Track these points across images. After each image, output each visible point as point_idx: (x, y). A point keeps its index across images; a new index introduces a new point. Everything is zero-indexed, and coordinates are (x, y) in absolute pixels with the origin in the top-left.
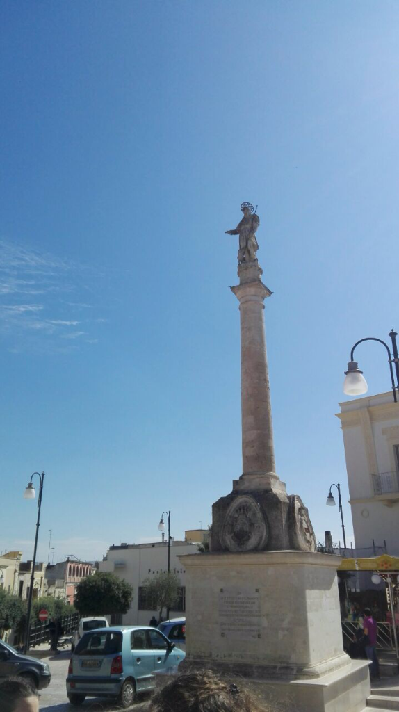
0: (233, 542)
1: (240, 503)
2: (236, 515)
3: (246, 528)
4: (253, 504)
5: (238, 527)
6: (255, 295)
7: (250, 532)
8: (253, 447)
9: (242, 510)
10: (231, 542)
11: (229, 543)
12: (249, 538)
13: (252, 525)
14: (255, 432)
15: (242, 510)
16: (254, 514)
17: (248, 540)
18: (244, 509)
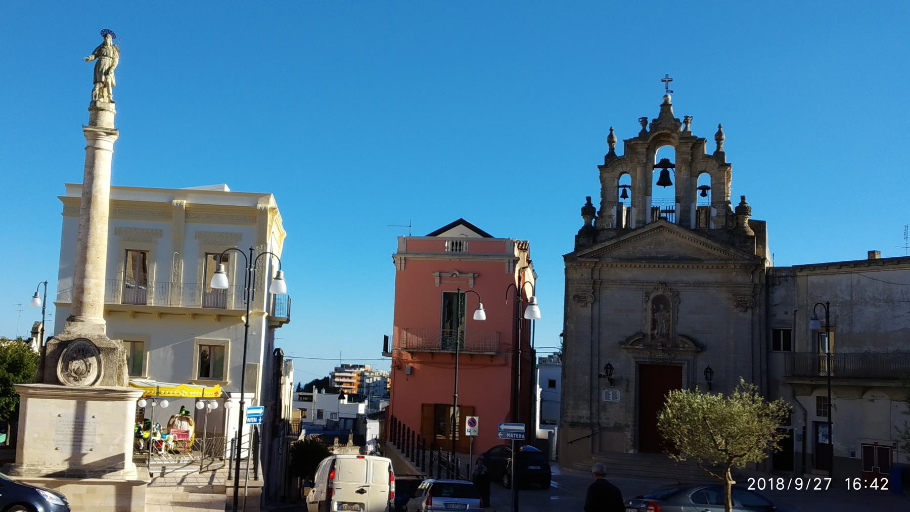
1: (78, 345)
9: (81, 352)
15: (81, 352)
18: (83, 351)
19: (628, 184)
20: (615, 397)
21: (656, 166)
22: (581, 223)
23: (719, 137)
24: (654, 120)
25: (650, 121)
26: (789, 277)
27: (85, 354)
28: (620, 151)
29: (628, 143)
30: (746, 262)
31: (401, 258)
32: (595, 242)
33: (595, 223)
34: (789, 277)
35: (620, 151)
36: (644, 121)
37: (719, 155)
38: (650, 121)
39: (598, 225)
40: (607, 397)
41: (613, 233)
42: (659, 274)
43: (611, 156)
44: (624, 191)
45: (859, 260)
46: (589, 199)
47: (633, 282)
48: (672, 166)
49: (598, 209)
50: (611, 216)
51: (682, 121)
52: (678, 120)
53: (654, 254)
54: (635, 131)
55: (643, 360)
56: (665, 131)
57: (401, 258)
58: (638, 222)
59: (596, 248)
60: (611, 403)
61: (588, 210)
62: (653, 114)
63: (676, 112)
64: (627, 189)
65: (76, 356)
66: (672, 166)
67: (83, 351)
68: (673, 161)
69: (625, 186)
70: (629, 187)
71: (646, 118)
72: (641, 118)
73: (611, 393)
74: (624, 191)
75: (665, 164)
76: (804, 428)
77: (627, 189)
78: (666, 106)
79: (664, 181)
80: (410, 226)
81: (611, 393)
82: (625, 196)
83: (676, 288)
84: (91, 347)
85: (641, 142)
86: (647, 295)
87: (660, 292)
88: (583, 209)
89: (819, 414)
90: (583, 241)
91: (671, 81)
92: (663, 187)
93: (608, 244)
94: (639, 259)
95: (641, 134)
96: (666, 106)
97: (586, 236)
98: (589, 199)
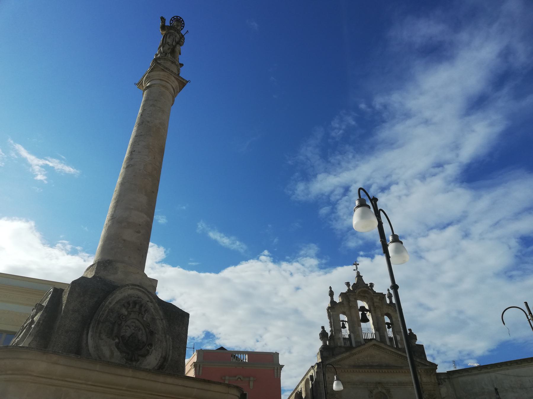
0: (117, 353)
2: (124, 312)
3: (142, 336)
4: (150, 304)
5: (127, 332)
6: (174, 90)
7: (151, 345)
8: (138, 232)
9: (137, 307)
10: (112, 353)
12: (148, 353)
13: (152, 333)
14: (145, 216)
16: (153, 319)
17: (144, 356)
18: (141, 306)
21: (360, 310)
22: (320, 344)
25: (351, 284)
26: (446, 379)
27: (143, 313)
28: (337, 299)
29: (342, 295)
30: (428, 367)
31: (200, 365)
32: (334, 355)
34: (446, 379)
36: (348, 284)
38: (351, 284)
39: (332, 344)
42: (376, 377)
43: (333, 302)
44: (343, 324)
45: (497, 363)
46: (323, 328)
48: (367, 311)
49: (329, 334)
51: (369, 285)
52: (367, 284)
54: (345, 289)
56: (365, 289)
57: (200, 365)
58: (356, 342)
59: (338, 358)
61: (323, 335)
62: (353, 281)
63: (367, 281)
64: (345, 323)
65: (126, 313)
66: (367, 311)
67: (141, 306)
68: (367, 307)
69: (343, 321)
70: (346, 321)
71: (349, 282)
72: (346, 283)
75: (363, 309)
77: (345, 323)
78: (359, 277)
79: (366, 320)
80: (194, 348)
84: (150, 304)
85: (352, 294)
86: (371, 392)
87: (380, 389)
88: (321, 334)
91: (359, 265)
93: (344, 355)
95: (349, 290)
96: (359, 277)
97: (325, 352)
98: (323, 328)
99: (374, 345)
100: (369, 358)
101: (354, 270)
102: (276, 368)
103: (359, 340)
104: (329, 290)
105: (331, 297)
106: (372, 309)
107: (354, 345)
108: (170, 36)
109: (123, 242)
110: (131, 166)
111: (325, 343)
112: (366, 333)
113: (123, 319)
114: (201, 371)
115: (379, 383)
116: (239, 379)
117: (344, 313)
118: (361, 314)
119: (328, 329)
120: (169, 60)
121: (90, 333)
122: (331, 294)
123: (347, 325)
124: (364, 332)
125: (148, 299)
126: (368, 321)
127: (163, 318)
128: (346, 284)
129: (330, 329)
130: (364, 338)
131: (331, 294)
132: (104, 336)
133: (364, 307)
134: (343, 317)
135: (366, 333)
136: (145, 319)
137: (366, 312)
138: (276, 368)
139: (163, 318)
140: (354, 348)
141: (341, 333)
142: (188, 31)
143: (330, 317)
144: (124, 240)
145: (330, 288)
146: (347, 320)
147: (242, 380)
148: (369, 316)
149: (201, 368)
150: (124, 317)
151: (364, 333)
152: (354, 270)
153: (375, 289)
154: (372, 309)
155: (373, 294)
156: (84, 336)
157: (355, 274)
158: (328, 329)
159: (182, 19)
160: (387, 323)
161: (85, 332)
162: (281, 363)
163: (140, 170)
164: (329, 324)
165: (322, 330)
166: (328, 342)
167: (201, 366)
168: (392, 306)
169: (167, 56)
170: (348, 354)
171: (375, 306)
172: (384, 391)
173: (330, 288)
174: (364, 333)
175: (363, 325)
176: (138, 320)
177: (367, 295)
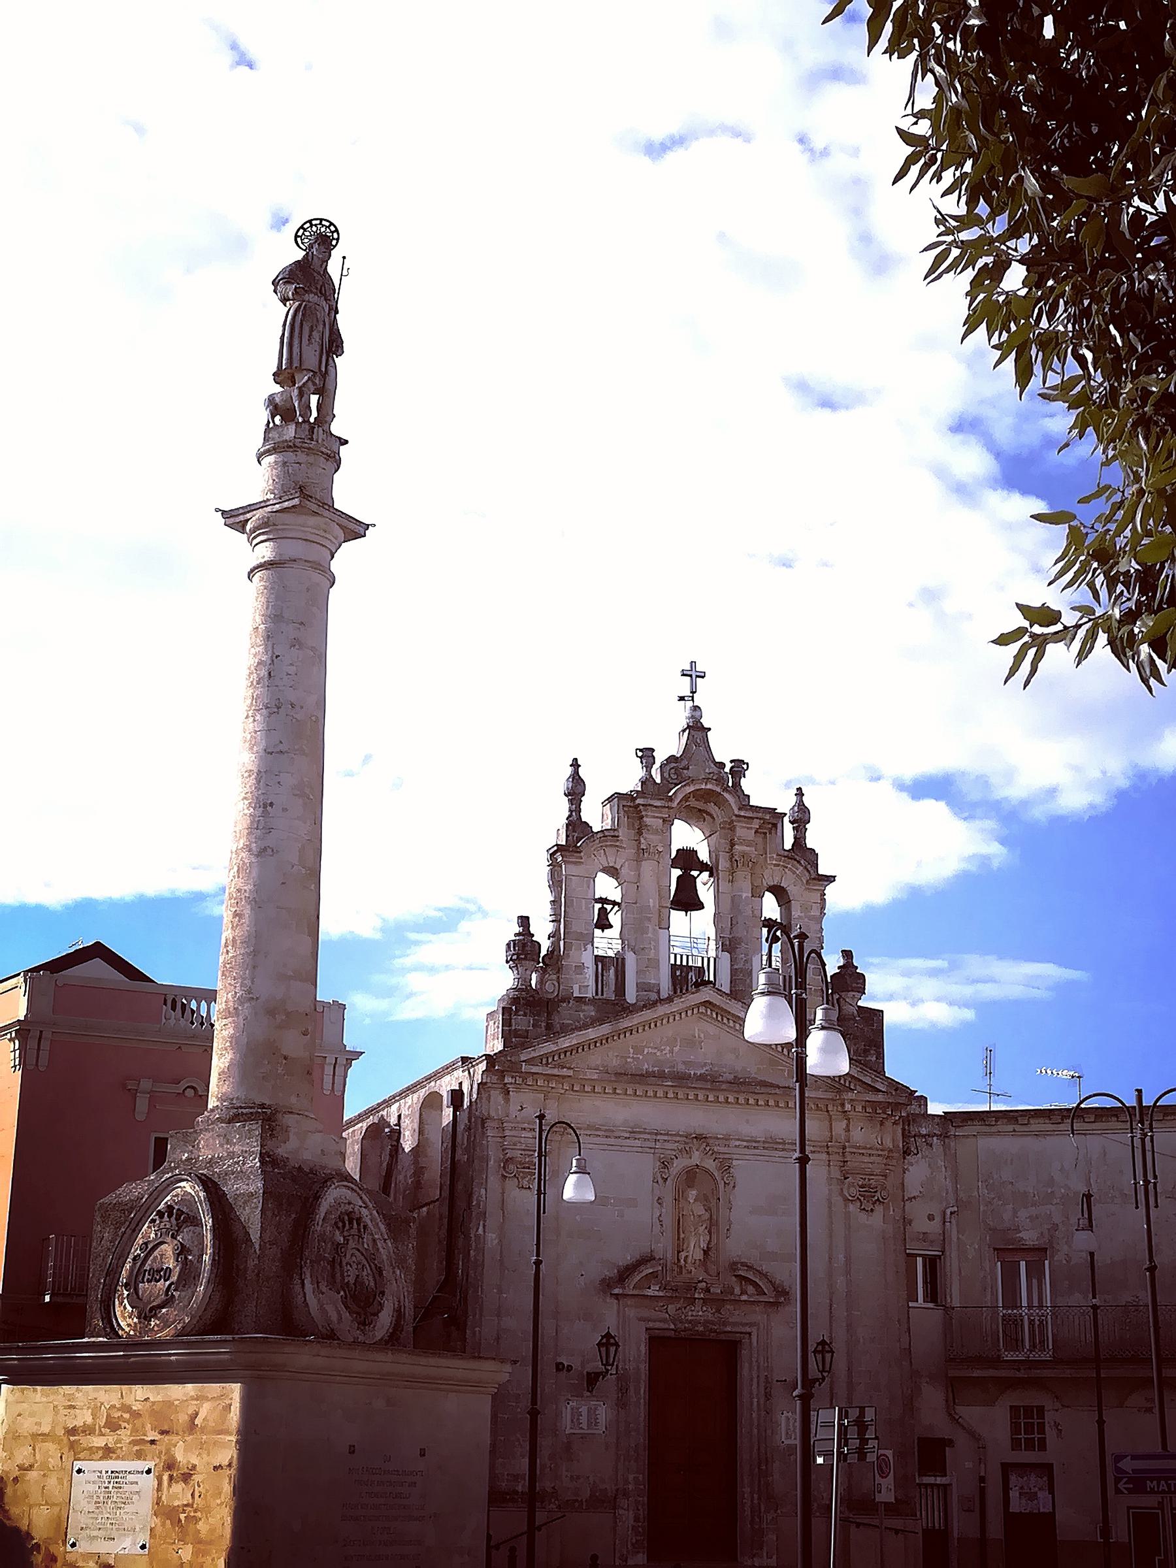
4: (365, 1212)
11: (334, 1317)
17: (376, 1314)
19: (611, 898)
20: (593, 1421)
22: (504, 980)
23: (801, 818)
24: (672, 759)
25: (660, 757)
26: (935, 1138)
28: (595, 815)
29: (620, 801)
30: (880, 1097)
32: (552, 1032)
33: (541, 981)
34: (935, 1138)
35: (595, 815)
36: (646, 755)
37: (804, 855)
38: (660, 757)
39: (549, 986)
40: (576, 1414)
41: (590, 1010)
43: (576, 825)
46: (524, 921)
47: (634, 1132)
48: (703, 867)
49: (543, 952)
50: (580, 968)
52: (722, 765)
53: (681, 1068)
54: (629, 778)
55: (662, 1325)
56: (709, 786)
58: (641, 987)
59: (565, 1042)
60: (583, 1437)
62: (669, 745)
63: (723, 750)
66: (703, 867)
68: (704, 855)
70: (614, 903)
71: (653, 750)
73: (584, 1410)
74: (603, 913)
75: (687, 859)
76: (982, 1479)
78: (696, 730)
79: (688, 901)
81: (584, 1410)
82: (604, 924)
83: (725, 1150)
86: (665, 1165)
87: (696, 1158)
89: (1016, 1445)
90: (522, 1022)
92: (684, 913)
93: (592, 1033)
94: (641, 1077)
95: (647, 781)
96: (696, 730)
98: (524, 921)
99: (707, 1004)
100: (676, 1049)
101: (682, 699)
102: (331, 1060)
103: (653, 981)
104: (569, 771)
105: (571, 801)
106: (723, 864)
107: (631, 996)
108: (311, 330)
109: (284, 1061)
110: (269, 850)
111: (524, 980)
112: (682, 956)
113: (342, 1253)
114: (44, 1055)
115: (699, 1137)
116: (190, 1092)
117: (612, 872)
118: (679, 878)
119: (542, 931)
120: (322, 452)
121: (309, 1286)
122: (576, 790)
123: (615, 918)
124: (677, 950)
125: (361, 1203)
126: (699, 906)
127: (386, 1237)
128: (640, 754)
129: (550, 928)
130: (672, 962)
131: (576, 790)
132: (324, 1289)
133: (694, 852)
134: (606, 887)
135: (682, 956)
136: (366, 1246)
137: (695, 873)
138: (331, 1060)
139: (386, 1237)
140: (630, 1010)
141: (589, 946)
142: (344, 258)
143: (555, 882)
144: (285, 1058)
145: (575, 764)
146: (619, 900)
147: (201, 1096)
148: (705, 890)
149: (45, 1045)
150: (343, 1250)
151: (675, 955)
152: (682, 699)
153: (747, 784)
154: (723, 864)
155: (736, 812)
156: (298, 1288)
157: (680, 716)
158: (542, 931)
159: (335, 226)
160: (769, 923)
161: (297, 1281)
162: (351, 1041)
163: (293, 866)
164: (547, 909)
165: (517, 929)
166: (534, 976)
167: (47, 1034)
168: (799, 862)
169: (315, 437)
170: (605, 1029)
171: (736, 858)
172: (710, 1164)
173: (575, 764)
174: (675, 955)
175: (678, 918)
176: (359, 1250)
177: (712, 808)
